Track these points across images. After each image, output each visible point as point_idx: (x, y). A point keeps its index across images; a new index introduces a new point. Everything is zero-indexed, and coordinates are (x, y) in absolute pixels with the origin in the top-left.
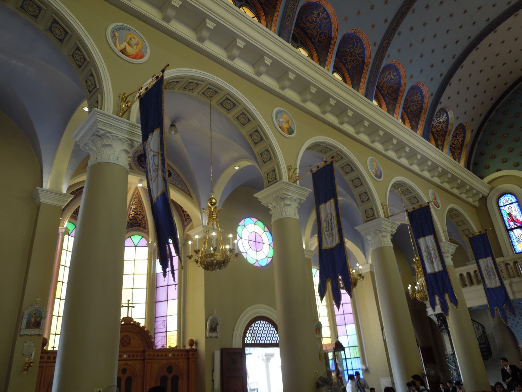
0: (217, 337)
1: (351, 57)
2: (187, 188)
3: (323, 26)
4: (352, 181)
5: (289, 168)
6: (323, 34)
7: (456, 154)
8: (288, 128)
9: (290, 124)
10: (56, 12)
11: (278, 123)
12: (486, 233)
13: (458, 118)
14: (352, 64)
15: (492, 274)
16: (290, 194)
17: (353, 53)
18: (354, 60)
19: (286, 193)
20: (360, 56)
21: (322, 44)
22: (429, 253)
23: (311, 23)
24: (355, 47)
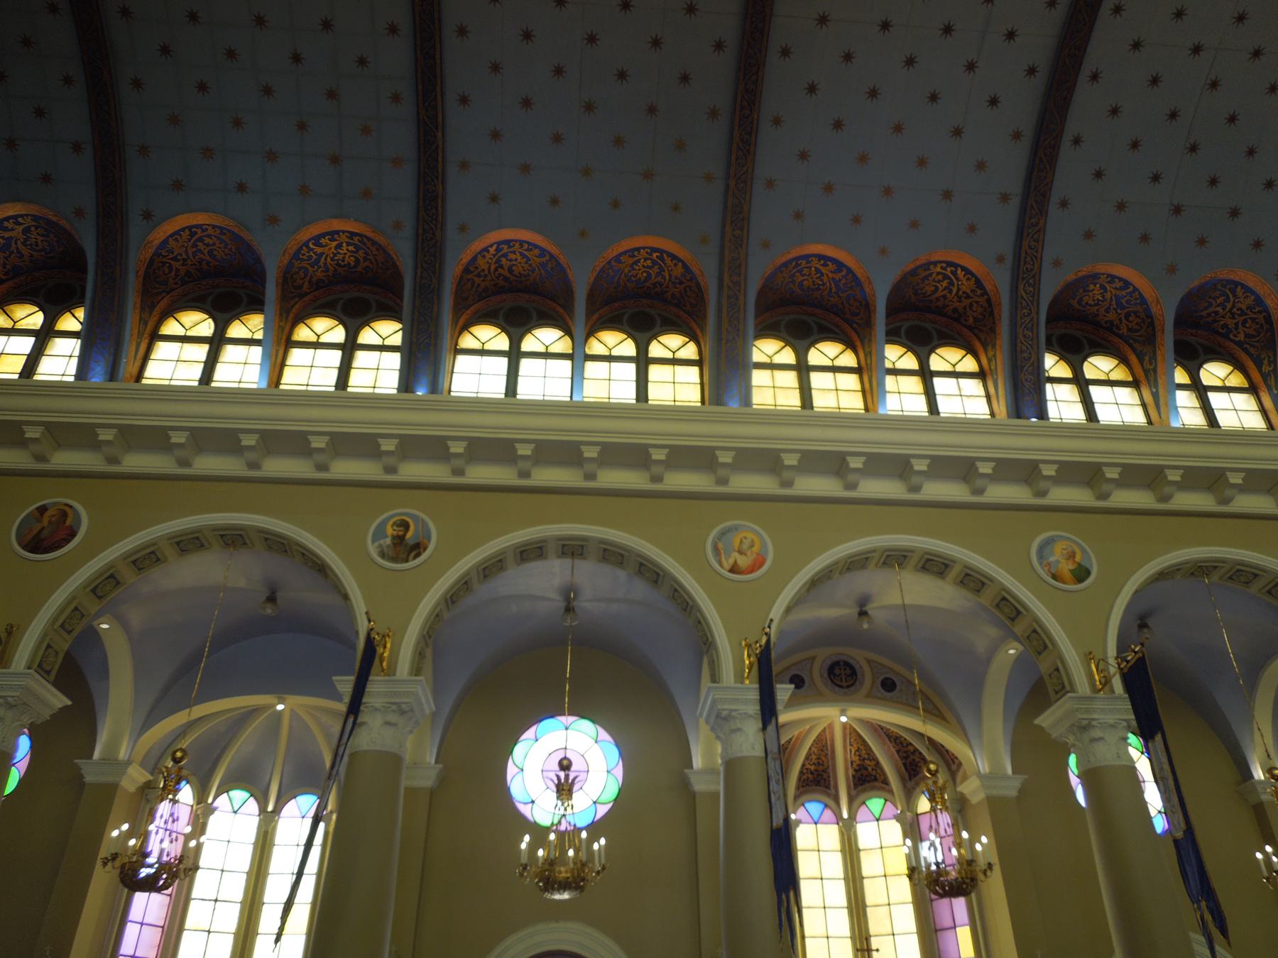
1: (1233, 318)
2: (933, 704)
3: (1124, 301)
5: (1088, 657)
6: (1132, 314)
8: (1073, 570)
9: (1078, 558)
10: (639, 555)
11: (1046, 569)
14: (1244, 331)
16: (1095, 716)
17: (1235, 310)
18: (1244, 322)
20: (1253, 310)
21: (1139, 334)
23: (1097, 305)
24: (1232, 299)
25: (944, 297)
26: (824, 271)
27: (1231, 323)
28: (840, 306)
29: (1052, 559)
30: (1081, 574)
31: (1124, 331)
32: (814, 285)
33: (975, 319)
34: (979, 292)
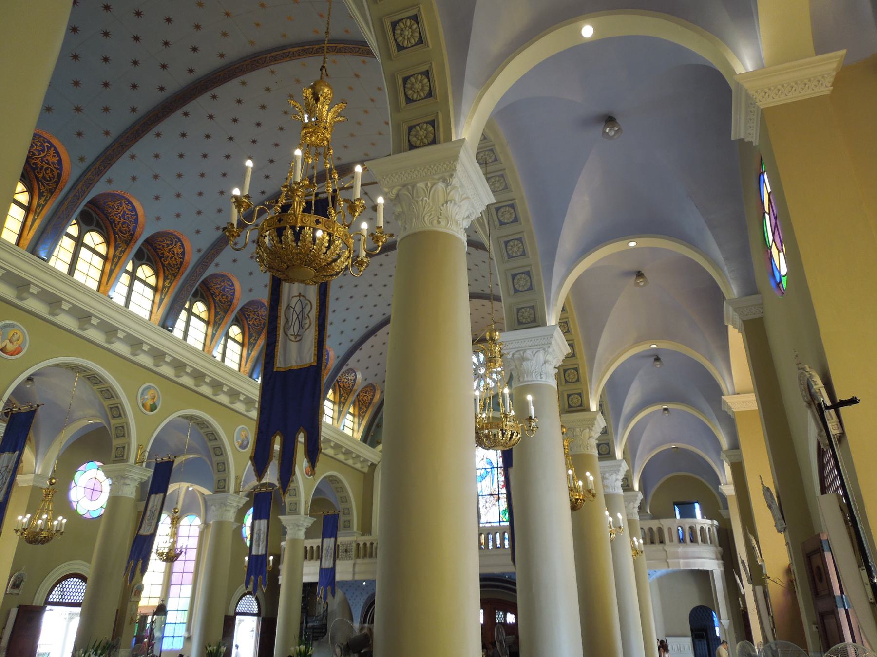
0: (18, 594)
3: (226, 290)
4: (214, 448)
7: (362, 411)
9: (155, 400)
11: (142, 400)
12: (338, 514)
13: (366, 379)
15: (329, 555)
17: (256, 313)
18: (256, 319)
19: (128, 473)
22: (259, 536)
24: (259, 308)
25: (163, 246)
26: (123, 206)
27: (252, 316)
28: (116, 222)
29: (146, 397)
30: (153, 408)
31: (217, 299)
32: (112, 206)
33: (169, 264)
34: (180, 256)
